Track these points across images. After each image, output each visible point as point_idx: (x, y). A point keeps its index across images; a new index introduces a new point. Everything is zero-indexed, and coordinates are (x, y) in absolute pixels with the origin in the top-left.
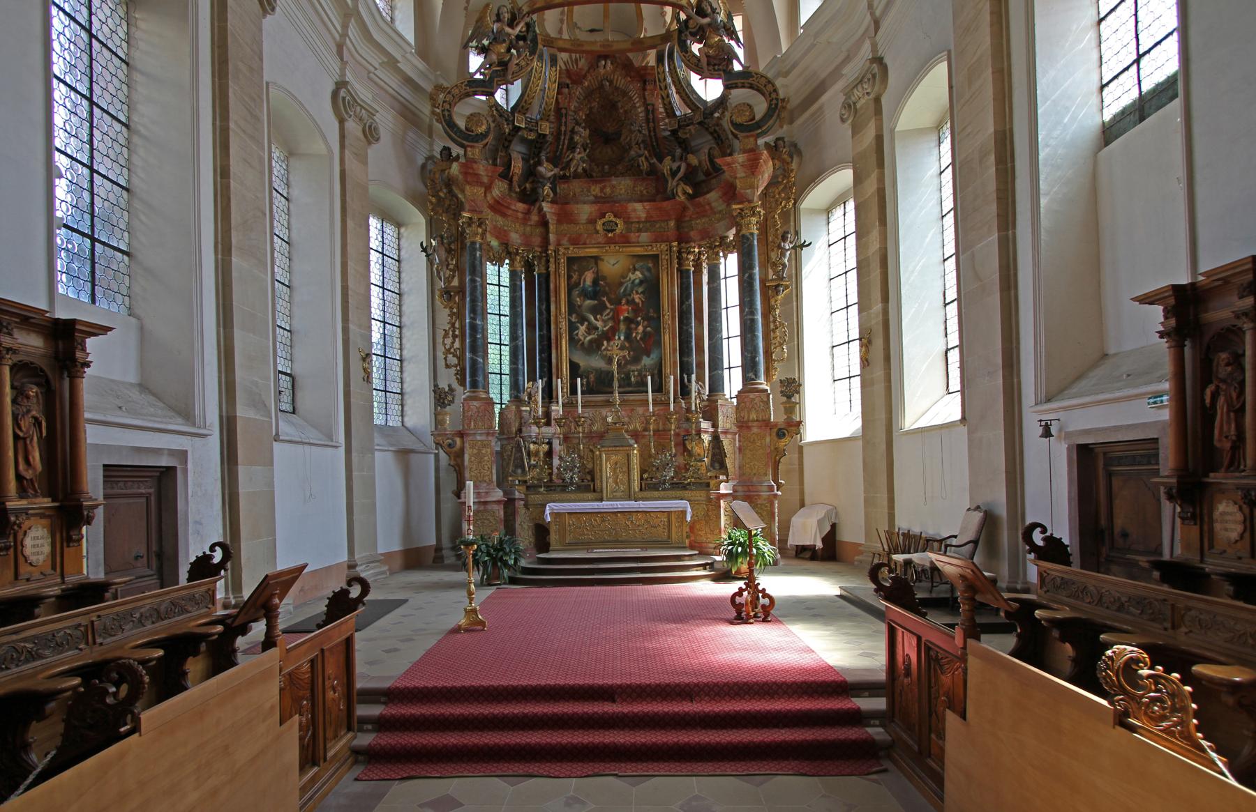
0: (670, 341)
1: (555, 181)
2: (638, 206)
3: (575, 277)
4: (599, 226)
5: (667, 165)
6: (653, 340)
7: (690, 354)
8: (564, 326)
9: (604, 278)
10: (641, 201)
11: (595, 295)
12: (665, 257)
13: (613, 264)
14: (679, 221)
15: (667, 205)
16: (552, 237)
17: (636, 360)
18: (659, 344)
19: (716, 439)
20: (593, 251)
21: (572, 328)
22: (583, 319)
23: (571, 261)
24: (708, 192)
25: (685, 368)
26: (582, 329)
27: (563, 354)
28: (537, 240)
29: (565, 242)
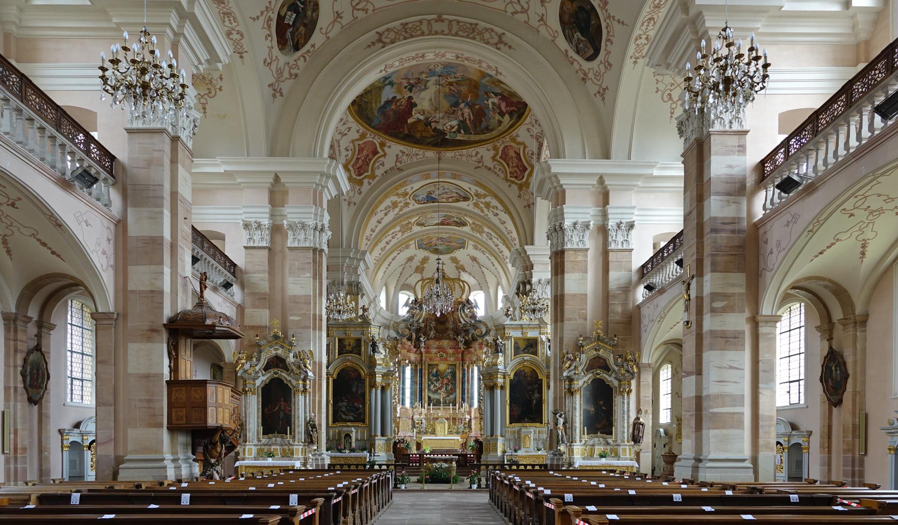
0: (458, 391)
1: (424, 342)
2: (450, 350)
3: (430, 370)
4: (438, 354)
5: (460, 338)
6: (453, 390)
7: (465, 395)
8: (427, 385)
9: (439, 371)
10: (451, 348)
11: (436, 376)
12: (458, 365)
13: (442, 367)
14: (463, 353)
15: (459, 350)
16: (424, 358)
17: (448, 396)
18: (455, 391)
19: (470, 420)
20: (436, 363)
21: (429, 386)
22: (432, 383)
23: (429, 365)
24: (471, 347)
25: (463, 399)
26: (432, 386)
27: (426, 394)
28: (419, 358)
29: (427, 359)
